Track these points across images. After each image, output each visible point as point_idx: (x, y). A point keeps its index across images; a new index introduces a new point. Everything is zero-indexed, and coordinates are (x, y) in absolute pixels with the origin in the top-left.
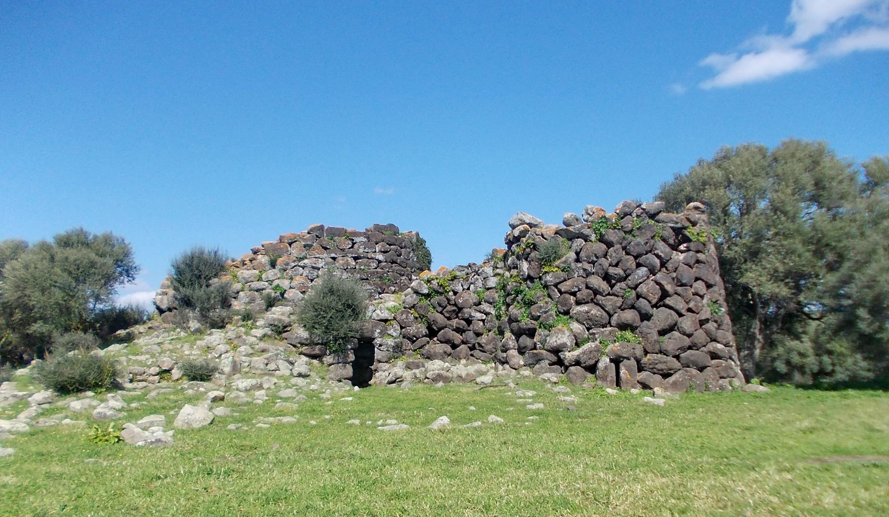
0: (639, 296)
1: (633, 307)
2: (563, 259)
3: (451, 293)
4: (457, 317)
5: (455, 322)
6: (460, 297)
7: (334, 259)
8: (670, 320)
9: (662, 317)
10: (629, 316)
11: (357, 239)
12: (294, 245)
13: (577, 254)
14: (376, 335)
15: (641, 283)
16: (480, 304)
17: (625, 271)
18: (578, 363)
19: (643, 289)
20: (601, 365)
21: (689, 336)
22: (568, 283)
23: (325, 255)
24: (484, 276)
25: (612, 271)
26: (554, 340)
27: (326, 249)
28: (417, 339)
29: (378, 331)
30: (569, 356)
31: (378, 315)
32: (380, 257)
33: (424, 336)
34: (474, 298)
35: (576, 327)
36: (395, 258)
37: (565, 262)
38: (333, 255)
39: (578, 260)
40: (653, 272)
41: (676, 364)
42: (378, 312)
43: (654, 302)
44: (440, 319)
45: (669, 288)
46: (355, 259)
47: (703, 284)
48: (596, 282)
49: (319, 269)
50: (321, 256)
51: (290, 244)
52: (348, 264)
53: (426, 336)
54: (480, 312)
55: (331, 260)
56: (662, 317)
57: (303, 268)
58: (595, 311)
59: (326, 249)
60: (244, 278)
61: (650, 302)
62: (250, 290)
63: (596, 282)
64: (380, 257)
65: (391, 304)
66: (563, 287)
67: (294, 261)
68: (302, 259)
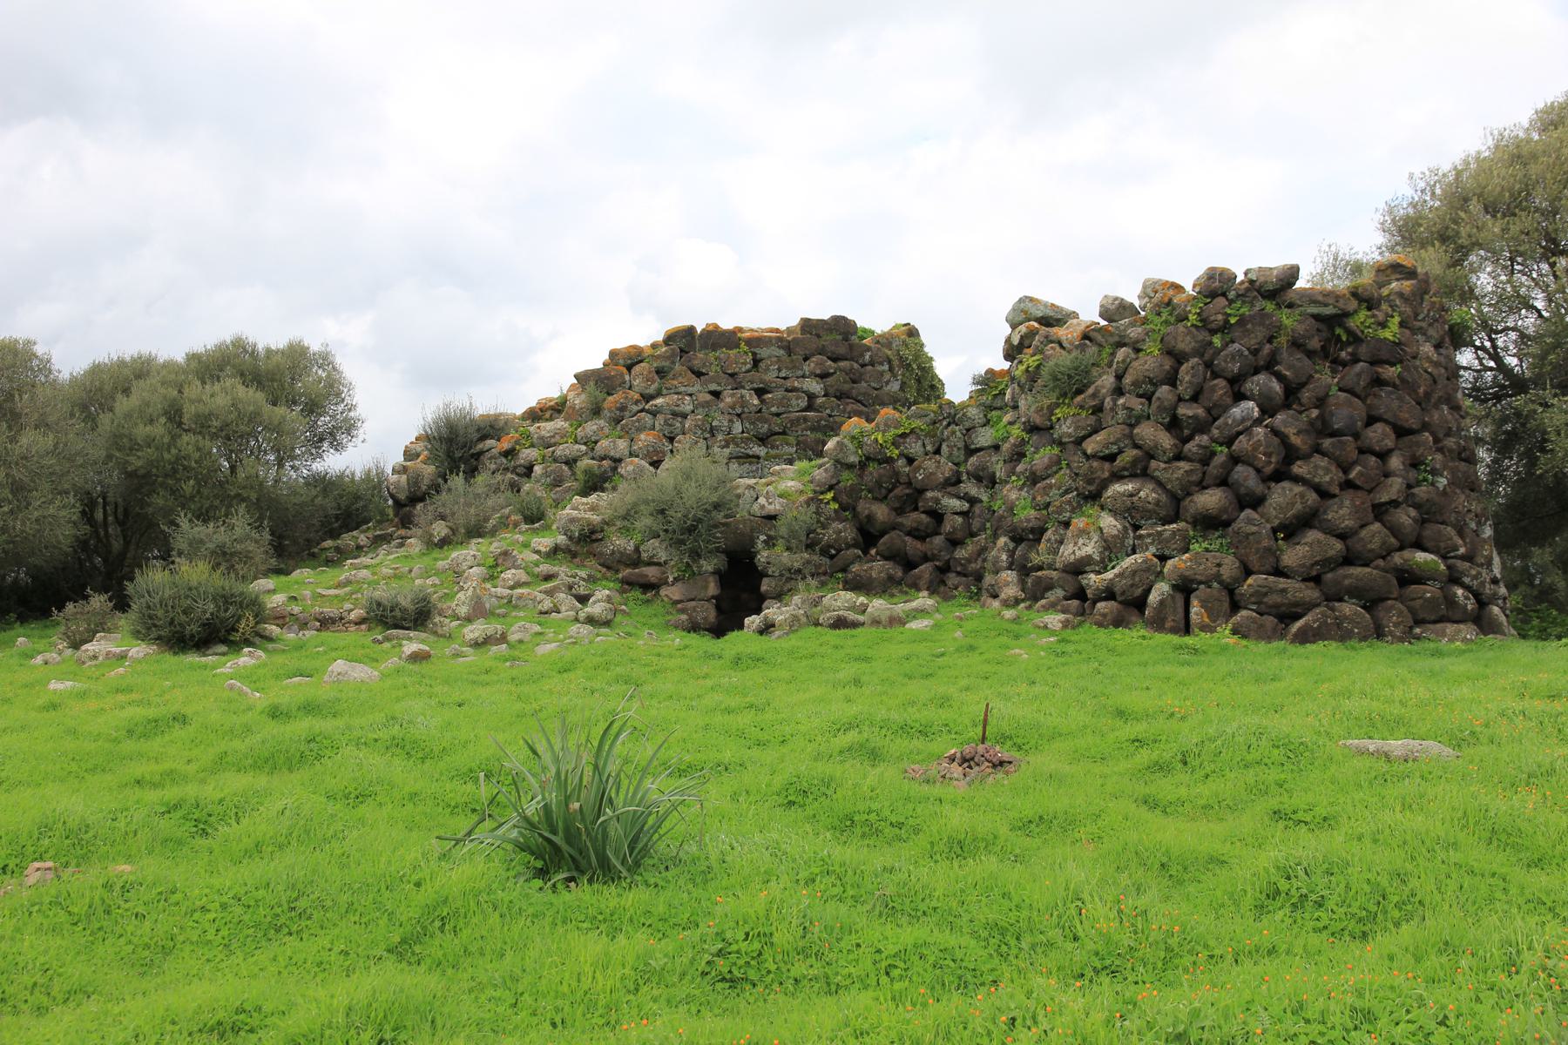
1: (1223, 482)
2: (1091, 391)
3: (902, 462)
4: (916, 509)
6: (919, 468)
7: (716, 394)
8: (1299, 506)
9: (1284, 499)
10: (1210, 500)
11: (763, 352)
12: (637, 369)
13: (1119, 377)
14: (760, 545)
15: (1239, 433)
16: (959, 481)
17: (1208, 410)
18: (1109, 594)
19: (1242, 444)
20: (1154, 598)
21: (1342, 537)
22: (1099, 437)
23: (697, 387)
24: (967, 425)
25: (1185, 411)
26: (1072, 551)
28: (839, 551)
29: (763, 538)
30: (1093, 580)
31: (763, 507)
32: (815, 386)
33: (848, 547)
34: (947, 468)
35: (1109, 523)
36: (846, 387)
37: (1094, 396)
38: (713, 387)
39: (1119, 391)
40: (1267, 410)
41: (1310, 593)
42: (762, 500)
43: (1268, 470)
44: (881, 512)
45: (1296, 440)
46: (760, 392)
47: (1388, 429)
48: (1151, 433)
49: (684, 416)
50: (690, 390)
51: (629, 368)
52: (743, 402)
53: (856, 546)
54: (959, 498)
55: (709, 397)
56: (1284, 499)
57: (654, 414)
58: (1148, 493)
59: (699, 374)
60: (542, 438)
61: (1258, 471)
62: (555, 460)
63: (1151, 433)
64: (815, 386)
65: (790, 485)
66: (1090, 446)
67: (637, 402)
68: (652, 397)
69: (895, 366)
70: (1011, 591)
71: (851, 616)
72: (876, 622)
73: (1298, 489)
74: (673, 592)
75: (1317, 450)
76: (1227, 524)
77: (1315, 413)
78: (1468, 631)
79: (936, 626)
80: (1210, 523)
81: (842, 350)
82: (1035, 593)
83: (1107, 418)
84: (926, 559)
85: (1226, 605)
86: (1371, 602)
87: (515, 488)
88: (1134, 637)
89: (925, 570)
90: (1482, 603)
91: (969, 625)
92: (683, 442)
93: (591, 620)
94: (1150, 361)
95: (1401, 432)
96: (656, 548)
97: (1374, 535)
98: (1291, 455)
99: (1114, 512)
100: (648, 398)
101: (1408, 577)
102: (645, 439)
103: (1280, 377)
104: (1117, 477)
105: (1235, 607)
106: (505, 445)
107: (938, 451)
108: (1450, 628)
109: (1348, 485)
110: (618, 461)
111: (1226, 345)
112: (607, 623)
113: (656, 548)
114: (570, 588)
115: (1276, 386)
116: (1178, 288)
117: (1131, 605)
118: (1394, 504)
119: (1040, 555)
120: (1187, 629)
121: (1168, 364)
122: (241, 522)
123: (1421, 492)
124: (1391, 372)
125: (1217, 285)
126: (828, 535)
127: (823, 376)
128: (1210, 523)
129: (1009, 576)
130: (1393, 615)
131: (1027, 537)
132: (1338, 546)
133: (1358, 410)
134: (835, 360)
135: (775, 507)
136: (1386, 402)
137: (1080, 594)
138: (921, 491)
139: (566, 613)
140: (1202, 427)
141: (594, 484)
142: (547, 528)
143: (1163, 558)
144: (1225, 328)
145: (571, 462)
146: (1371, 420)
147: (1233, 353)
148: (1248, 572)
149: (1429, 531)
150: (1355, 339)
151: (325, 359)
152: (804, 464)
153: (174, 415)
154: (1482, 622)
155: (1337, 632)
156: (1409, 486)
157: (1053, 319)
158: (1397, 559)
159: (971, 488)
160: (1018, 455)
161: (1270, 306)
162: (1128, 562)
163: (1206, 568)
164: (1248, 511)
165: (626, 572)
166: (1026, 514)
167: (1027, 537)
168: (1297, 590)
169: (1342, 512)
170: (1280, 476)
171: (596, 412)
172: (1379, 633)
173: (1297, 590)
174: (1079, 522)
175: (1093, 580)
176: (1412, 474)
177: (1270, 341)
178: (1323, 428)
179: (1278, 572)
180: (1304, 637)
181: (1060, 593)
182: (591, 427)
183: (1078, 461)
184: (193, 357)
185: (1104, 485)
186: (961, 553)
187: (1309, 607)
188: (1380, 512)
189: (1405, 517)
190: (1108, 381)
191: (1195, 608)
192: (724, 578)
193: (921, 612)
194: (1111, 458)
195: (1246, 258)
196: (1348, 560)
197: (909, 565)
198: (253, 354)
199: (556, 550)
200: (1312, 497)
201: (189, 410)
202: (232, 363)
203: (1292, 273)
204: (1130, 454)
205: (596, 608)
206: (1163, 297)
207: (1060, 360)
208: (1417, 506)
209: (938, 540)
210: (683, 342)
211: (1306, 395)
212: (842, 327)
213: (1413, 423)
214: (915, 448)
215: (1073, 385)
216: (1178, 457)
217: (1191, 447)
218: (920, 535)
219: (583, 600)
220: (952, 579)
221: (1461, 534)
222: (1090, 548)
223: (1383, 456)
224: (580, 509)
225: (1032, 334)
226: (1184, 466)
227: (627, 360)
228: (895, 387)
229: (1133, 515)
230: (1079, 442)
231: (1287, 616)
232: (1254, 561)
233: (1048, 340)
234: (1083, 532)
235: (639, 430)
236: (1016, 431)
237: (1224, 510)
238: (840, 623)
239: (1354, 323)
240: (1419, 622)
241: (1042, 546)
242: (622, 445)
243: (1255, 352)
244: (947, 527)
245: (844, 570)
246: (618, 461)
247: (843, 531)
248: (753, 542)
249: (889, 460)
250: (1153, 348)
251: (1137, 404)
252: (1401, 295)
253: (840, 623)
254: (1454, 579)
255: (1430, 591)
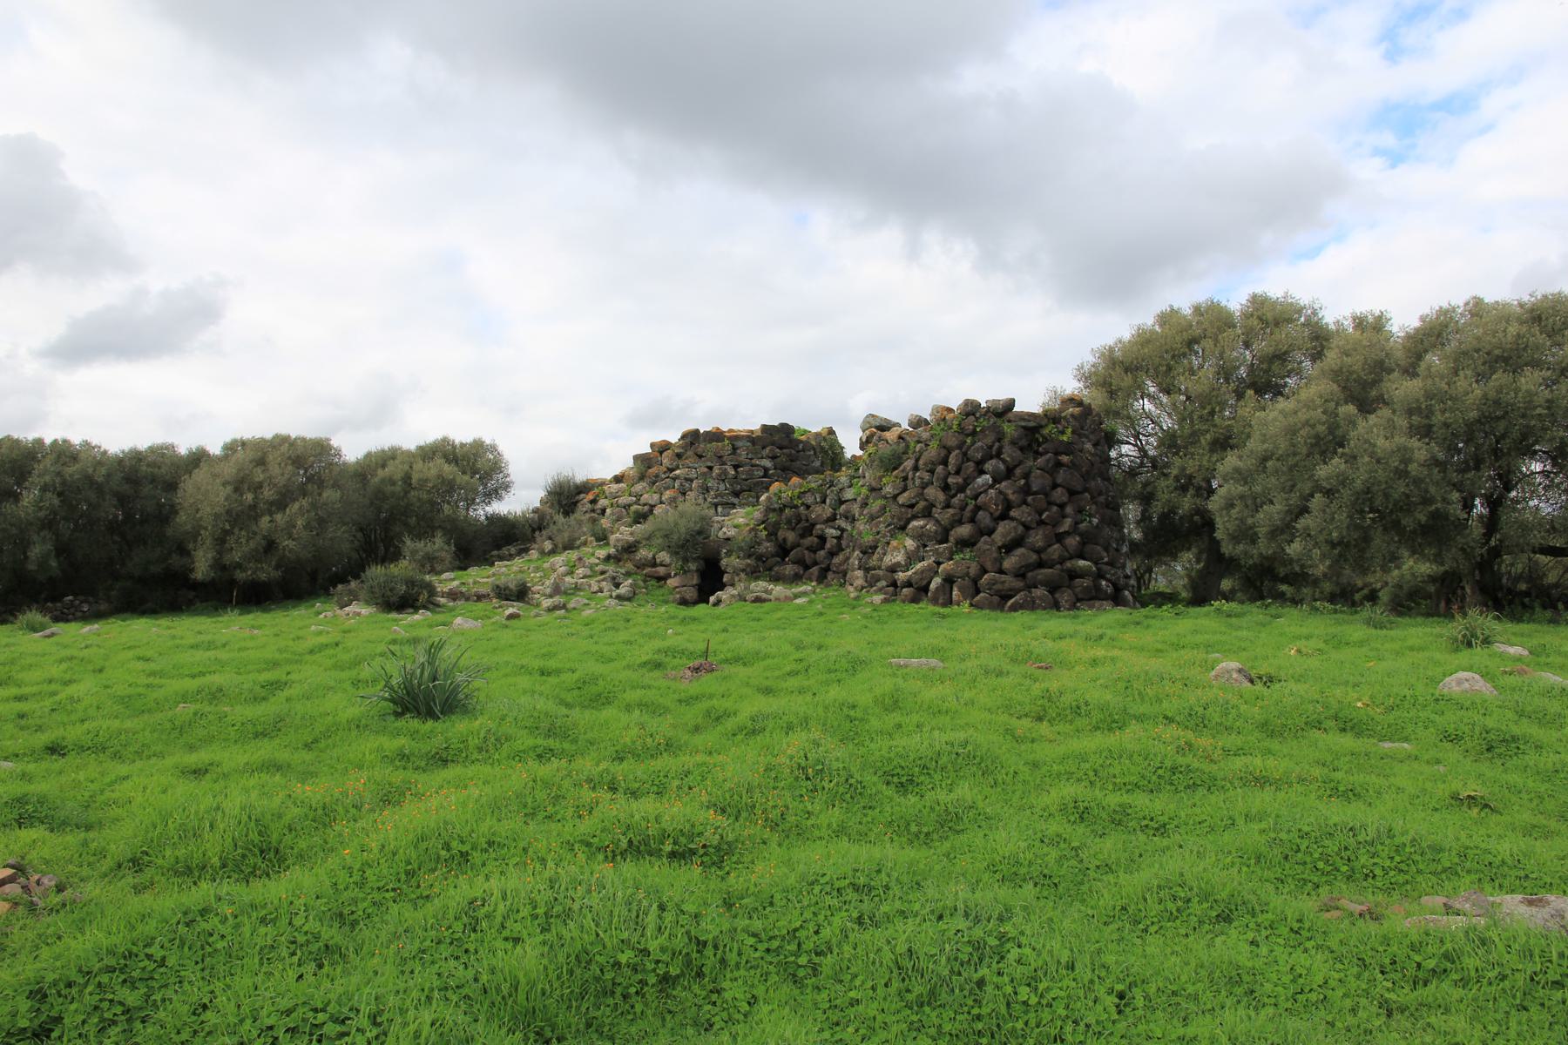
0: (978, 508)
1: (972, 520)
5: (811, 540)
9: (1004, 531)
10: (964, 530)
11: (739, 444)
13: (917, 460)
18: (909, 584)
19: (982, 499)
20: (933, 586)
21: (1038, 552)
26: (889, 560)
27: (700, 457)
32: (767, 463)
34: (829, 512)
35: (910, 543)
39: (916, 468)
40: (996, 480)
41: (1019, 584)
44: (791, 537)
45: (1011, 497)
46: (736, 467)
48: (934, 493)
49: (691, 480)
52: (725, 472)
56: (1004, 531)
58: (931, 527)
59: (700, 457)
64: (767, 463)
66: (901, 500)
69: (825, 451)
70: (860, 582)
71: (764, 596)
72: (777, 599)
73: (1014, 524)
74: (671, 582)
75: (1025, 502)
76: (974, 544)
77: (1023, 482)
78: (1107, 605)
79: (811, 602)
80: (964, 544)
81: (786, 443)
82: (871, 583)
83: (909, 482)
84: (815, 563)
85: (972, 590)
86: (1053, 588)
87: (594, 521)
88: (926, 608)
89: (815, 570)
90: (1118, 589)
91: (828, 601)
92: (691, 495)
93: (619, 597)
94: (933, 451)
95: (1072, 493)
96: (664, 556)
97: (1055, 550)
98: (1008, 506)
99: (913, 537)
100: (671, 470)
101: (1073, 575)
102: (668, 494)
103: (1004, 461)
104: (915, 517)
105: (978, 592)
106: (590, 497)
107: (824, 502)
108: (1097, 603)
109: (1041, 523)
110: (652, 507)
111: (973, 443)
112: (629, 599)
113: (664, 556)
114: (614, 578)
115: (1002, 466)
116: (950, 410)
117: (920, 591)
118: (1067, 533)
119: (873, 562)
120: (949, 602)
121: (943, 453)
122: (439, 541)
123: (1083, 526)
124: (1065, 459)
125: (971, 409)
126: (761, 550)
127: (773, 458)
128: (964, 544)
129: (859, 573)
130: (1065, 597)
131: (869, 551)
132: (1035, 557)
133: (1048, 481)
134: (781, 448)
135: (732, 532)
136: (1061, 476)
137: (894, 584)
138: (813, 525)
139: (606, 594)
140: (962, 489)
141: (640, 518)
142: (608, 544)
143: (939, 564)
144: (974, 433)
145: (627, 507)
146: (1055, 486)
147: (977, 449)
148: (986, 572)
149: (1089, 548)
150: (1046, 440)
151: (493, 448)
152: (749, 509)
153: (407, 479)
154: (1117, 600)
155: (1030, 605)
156: (1077, 523)
157: (884, 427)
158: (1068, 564)
159: (842, 523)
160: (865, 504)
161: (999, 422)
162: (919, 566)
163: (961, 570)
164: (985, 538)
165: (648, 570)
166: (868, 539)
167: (869, 551)
168: (1010, 581)
169: (1037, 538)
170: (1004, 516)
171: (642, 478)
172: (1056, 606)
173: (1010, 581)
174: (894, 543)
175: (901, 576)
176: (1079, 517)
177: (999, 440)
178: (1026, 491)
179: (1001, 572)
180: (1014, 608)
181: (884, 583)
182: (639, 487)
183: (894, 509)
184: (420, 448)
185: (908, 521)
186: (836, 560)
187: (1015, 592)
188: (1060, 538)
189: (1073, 542)
190: (909, 464)
191: (955, 592)
192: (703, 574)
193: (804, 594)
194: (912, 506)
195: (986, 394)
196: (1041, 565)
197: (807, 567)
198: (454, 447)
199: (608, 558)
200: (1021, 528)
201: (415, 477)
202: (443, 451)
203: (1011, 403)
204: (922, 504)
205: (623, 590)
206: (943, 413)
207: (885, 450)
208: (1081, 535)
209: (822, 553)
210: (692, 438)
211: (1018, 471)
212: (786, 429)
213: (1079, 488)
214: (809, 499)
215: (892, 463)
216: (948, 506)
217: (955, 501)
218: (813, 550)
219: (617, 586)
220: (830, 576)
221: (1106, 549)
222: (899, 558)
223: (1062, 506)
224: (623, 533)
225: (872, 435)
226: (951, 511)
227: (662, 448)
228: (817, 464)
229: (922, 538)
230: (895, 497)
231: (1005, 597)
232: (988, 565)
233: (880, 439)
234: (896, 548)
235: (667, 488)
236: (864, 491)
237: (971, 536)
238: (758, 600)
239: (1045, 431)
240: (1079, 600)
241: (876, 556)
242: (656, 497)
243: (991, 447)
244: (828, 545)
245: (770, 569)
246: (652, 507)
247: (767, 547)
248: (719, 553)
249: (796, 507)
250: (934, 444)
251: (927, 476)
252: (1072, 415)
253: (758, 600)
254: (1100, 575)
255: (1086, 582)
